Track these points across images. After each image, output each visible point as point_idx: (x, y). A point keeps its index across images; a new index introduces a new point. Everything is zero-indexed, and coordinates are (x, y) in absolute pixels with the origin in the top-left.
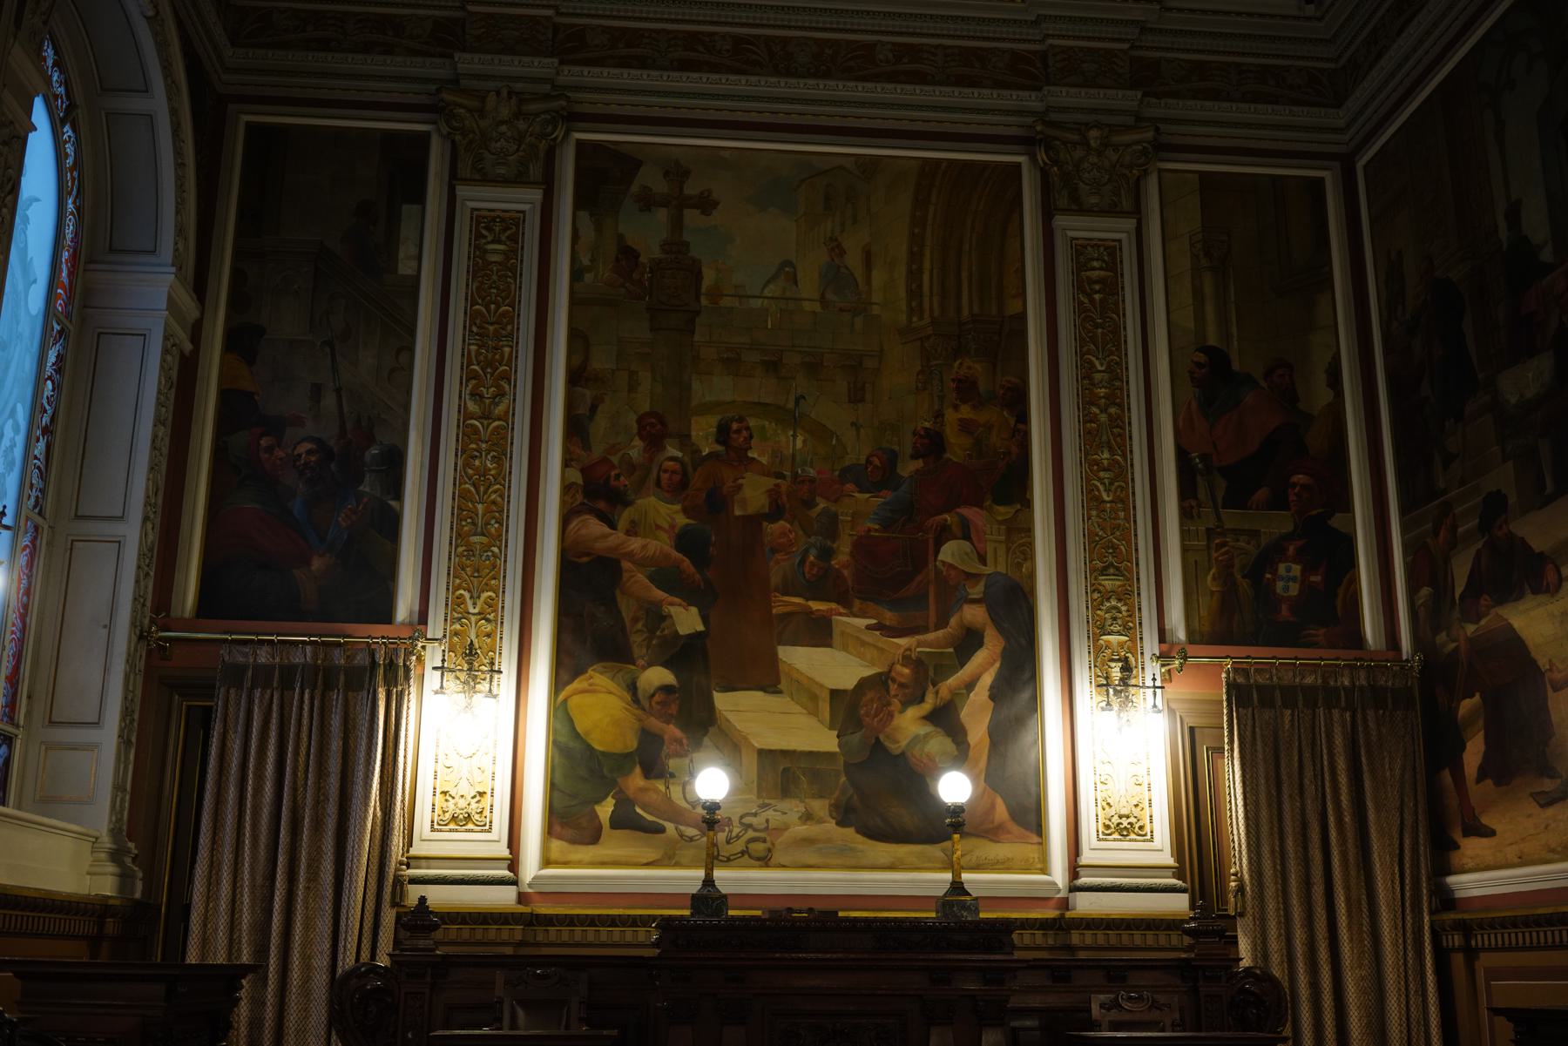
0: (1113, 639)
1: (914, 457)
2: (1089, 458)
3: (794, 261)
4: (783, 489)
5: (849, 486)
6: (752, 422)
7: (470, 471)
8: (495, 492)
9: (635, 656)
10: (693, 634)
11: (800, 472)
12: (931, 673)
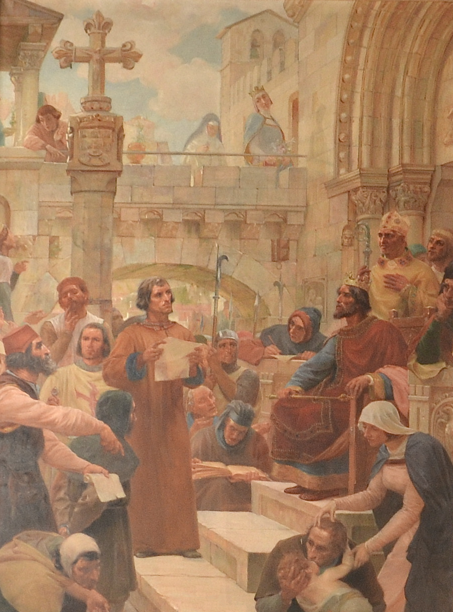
1: (338, 316)
3: (218, 115)
4: (204, 353)
6: (173, 285)
9: (58, 523)
10: (114, 501)
11: (221, 335)
12: (349, 536)
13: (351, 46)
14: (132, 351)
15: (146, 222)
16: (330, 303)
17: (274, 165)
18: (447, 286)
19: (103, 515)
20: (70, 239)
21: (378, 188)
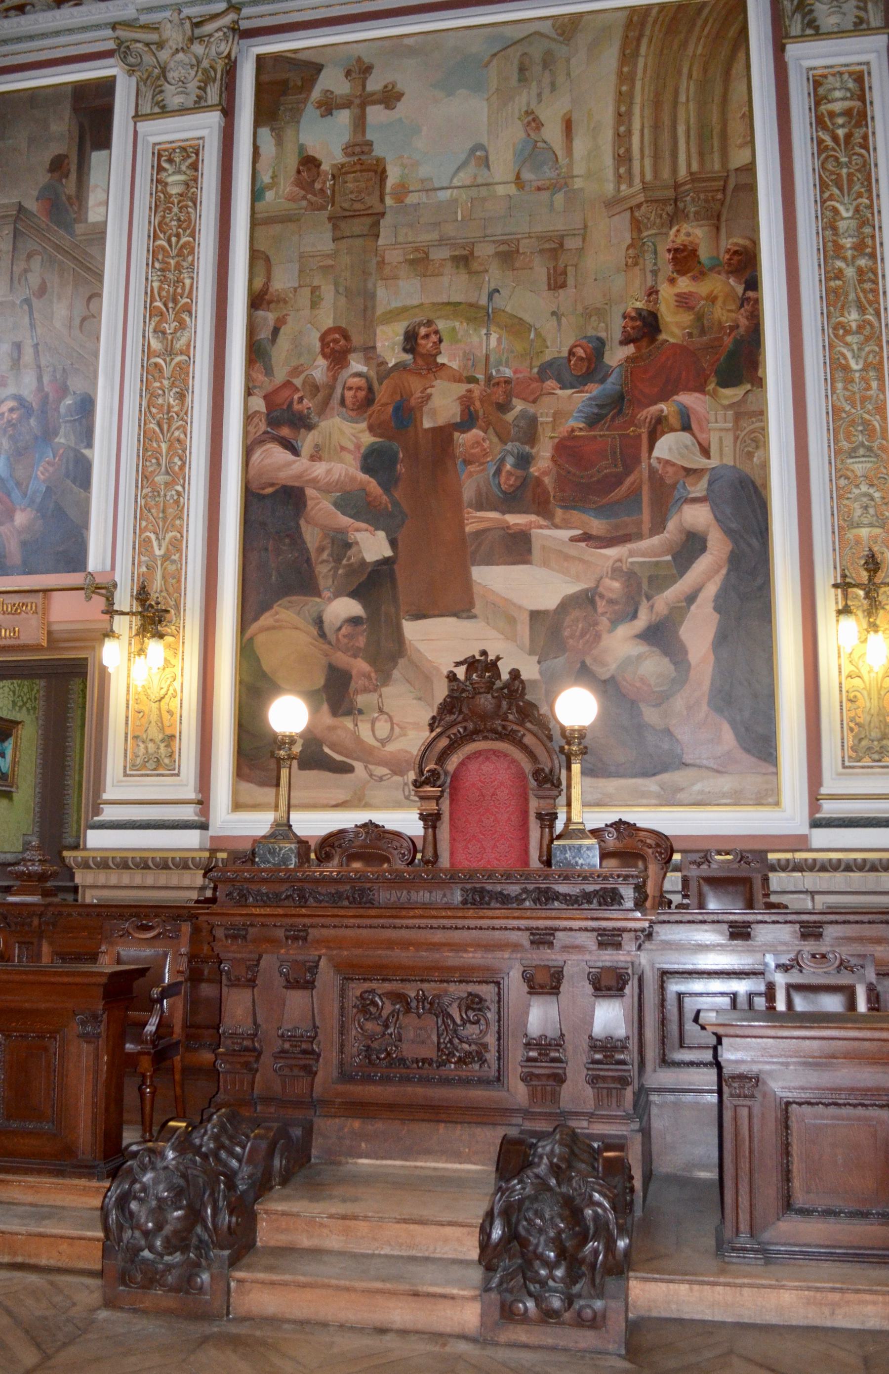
0: (864, 532)
1: (625, 342)
2: (833, 320)
3: (486, 144)
4: (477, 394)
5: (550, 383)
6: (441, 325)
7: (154, 410)
8: (178, 429)
9: (321, 588)
11: (494, 373)
12: (645, 586)
13: (628, 56)
14: (398, 398)
15: (412, 262)
16: (616, 327)
17: (548, 189)
18: (748, 299)
19: (369, 576)
20: (332, 287)
21: (665, 201)
